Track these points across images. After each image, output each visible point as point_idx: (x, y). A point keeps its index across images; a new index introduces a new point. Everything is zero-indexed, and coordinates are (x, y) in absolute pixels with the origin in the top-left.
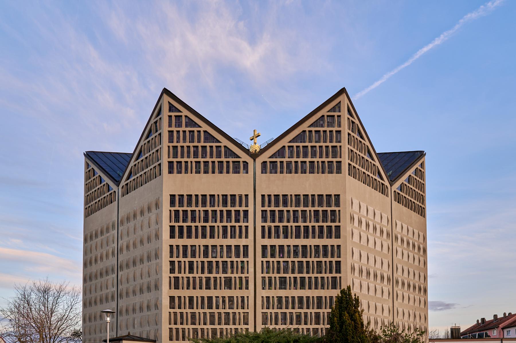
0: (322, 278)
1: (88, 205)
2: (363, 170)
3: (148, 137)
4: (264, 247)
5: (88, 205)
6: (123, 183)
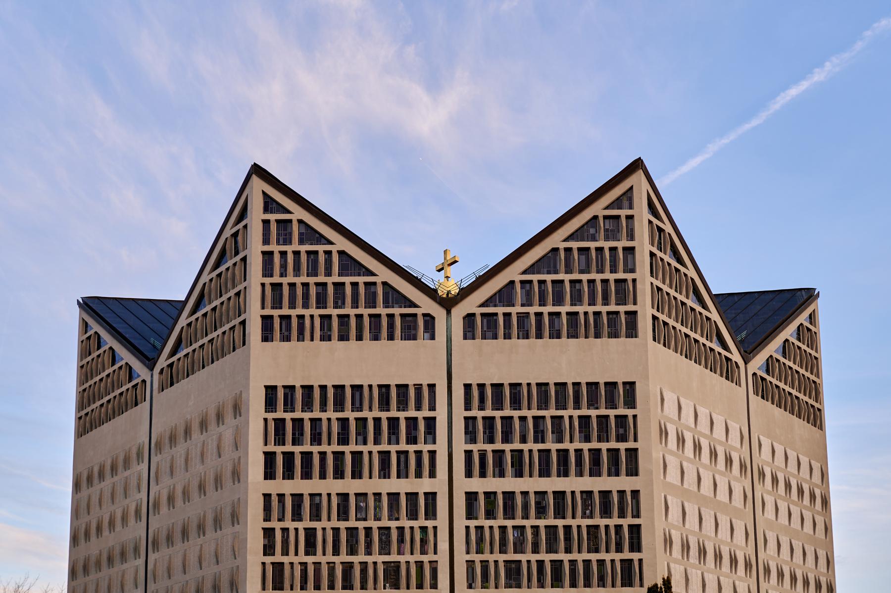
0: (601, 563)
1: (85, 411)
2: (684, 330)
3: (217, 265)
4: (471, 497)
5: (85, 411)
6: (162, 362)
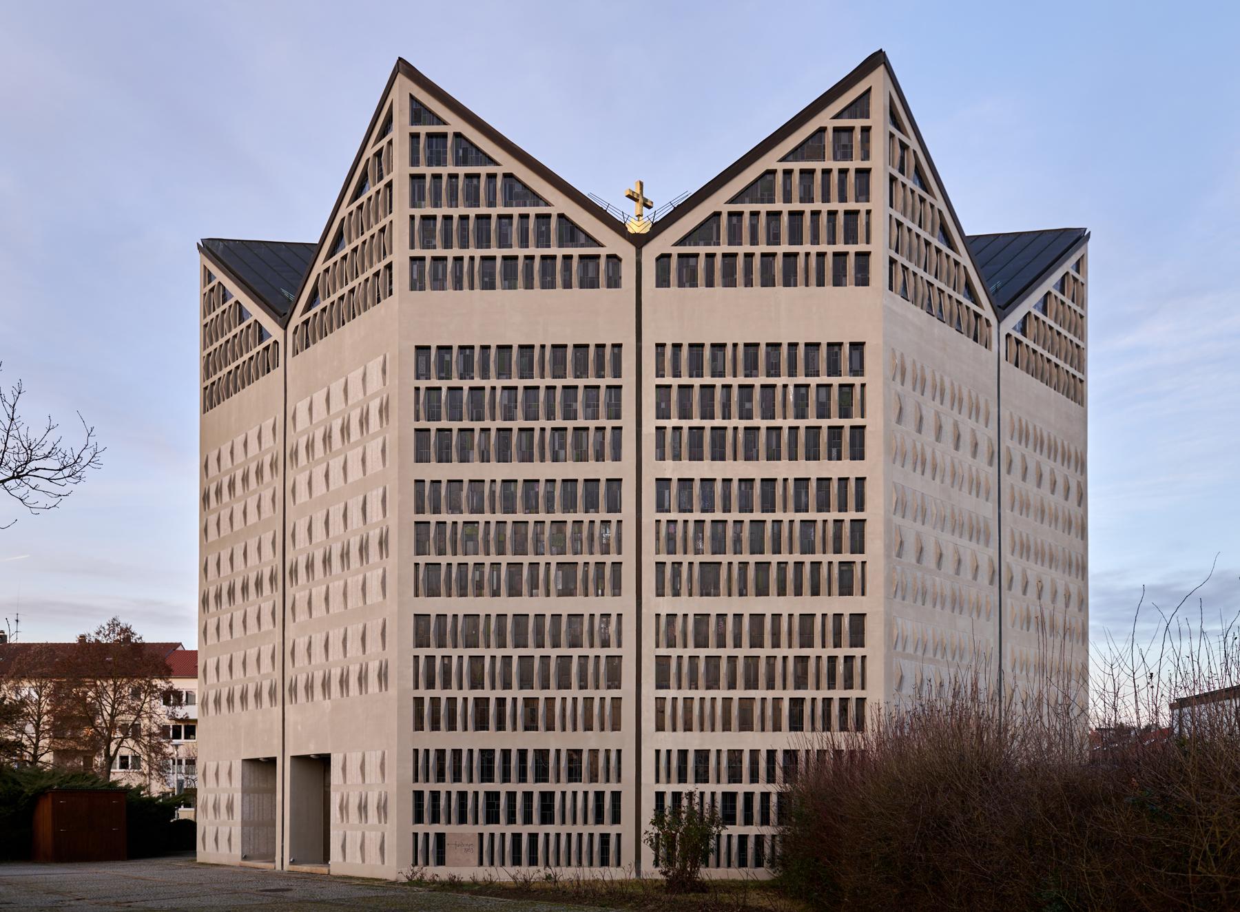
0: (816, 565)
1: (211, 380)
2: (927, 276)
3: (356, 196)
4: (663, 483)
5: (211, 380)
6: (297, 319)
